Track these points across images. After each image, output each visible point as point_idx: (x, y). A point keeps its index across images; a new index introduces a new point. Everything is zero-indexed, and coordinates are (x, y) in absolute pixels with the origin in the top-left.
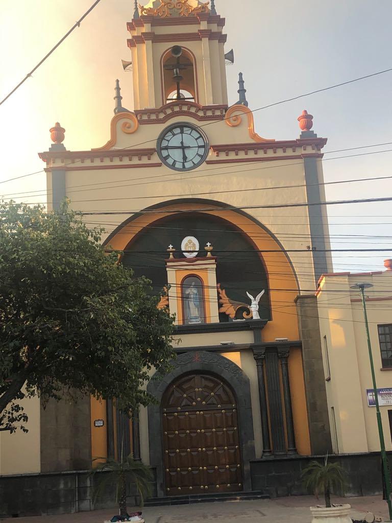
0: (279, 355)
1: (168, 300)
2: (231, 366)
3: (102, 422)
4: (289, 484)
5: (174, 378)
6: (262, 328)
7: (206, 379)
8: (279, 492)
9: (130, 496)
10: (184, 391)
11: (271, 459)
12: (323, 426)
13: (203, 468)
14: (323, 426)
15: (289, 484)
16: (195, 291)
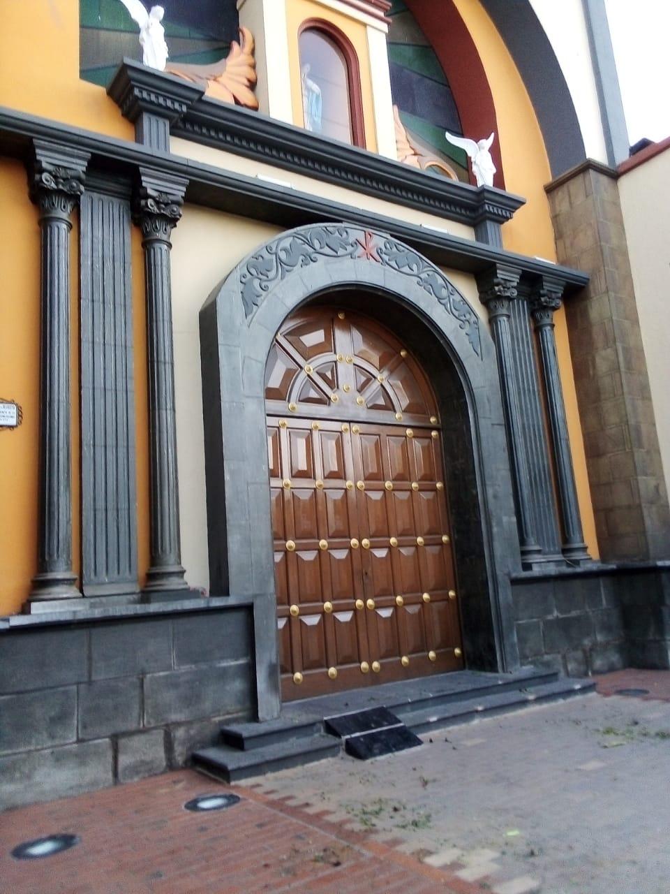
0: (543, 299)
1: (253, 67)
2: (452, 297)
3: (13, 411)
4: (587, 642)
5: (306, 291)
6: (502, 223)
7: (367, 333)
8: (570, 667)
9: (143, 731)
10: (308, 353)
11: (553, 573)
12: (657, 488)
13: (365, 603)
14: (657, 488)
15: (587, 642)
16: (315, 87)
